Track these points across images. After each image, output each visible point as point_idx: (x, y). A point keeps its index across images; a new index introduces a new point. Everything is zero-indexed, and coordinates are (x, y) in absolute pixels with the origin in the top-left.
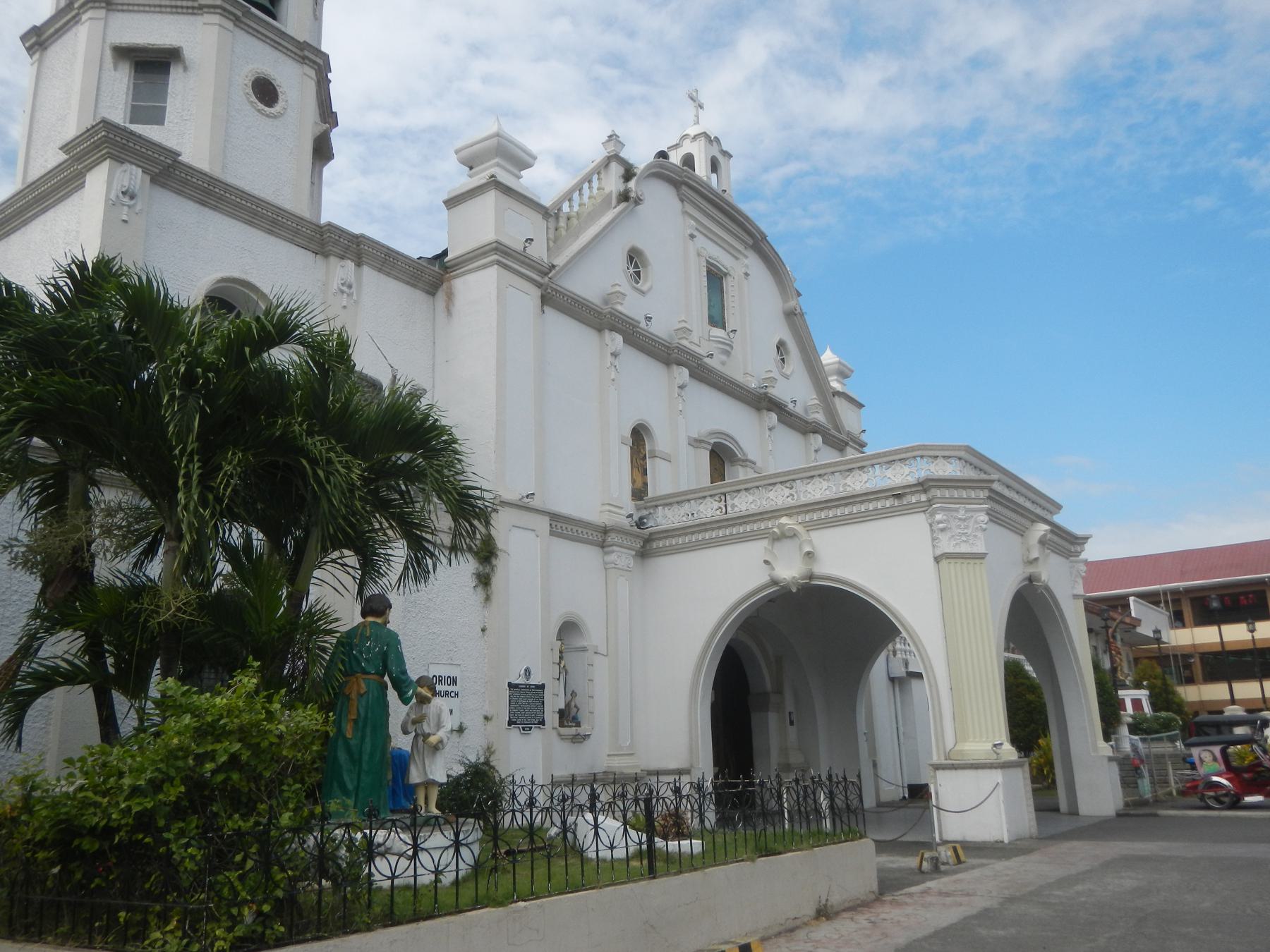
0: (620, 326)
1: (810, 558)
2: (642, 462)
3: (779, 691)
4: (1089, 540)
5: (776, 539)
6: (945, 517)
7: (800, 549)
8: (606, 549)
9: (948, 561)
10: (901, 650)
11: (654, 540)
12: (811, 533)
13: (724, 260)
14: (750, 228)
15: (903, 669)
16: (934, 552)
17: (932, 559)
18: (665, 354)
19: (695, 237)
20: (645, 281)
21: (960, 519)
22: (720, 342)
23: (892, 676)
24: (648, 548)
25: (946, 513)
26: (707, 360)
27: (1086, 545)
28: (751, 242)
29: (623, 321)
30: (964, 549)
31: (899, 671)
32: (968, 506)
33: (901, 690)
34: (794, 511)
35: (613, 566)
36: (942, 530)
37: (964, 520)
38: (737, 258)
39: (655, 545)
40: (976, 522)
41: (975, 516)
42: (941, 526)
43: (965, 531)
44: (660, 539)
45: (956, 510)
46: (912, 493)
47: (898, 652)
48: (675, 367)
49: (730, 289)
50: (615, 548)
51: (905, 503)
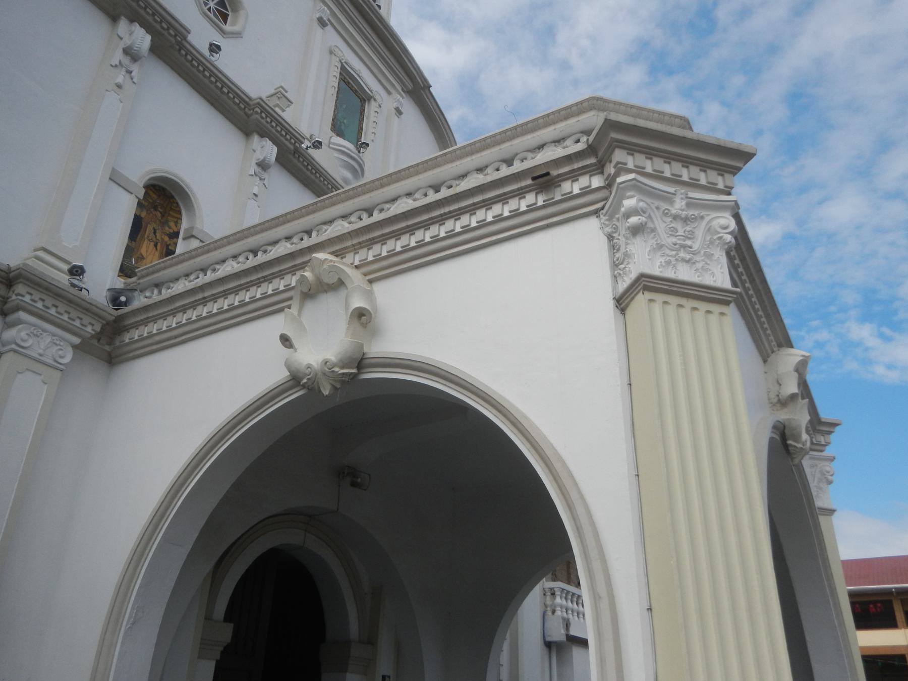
0: (150, 19)
1: (364, 325)
2: (166, 239)
3: (371, 641)
4: (837, 429)
5: (310, 294)
6: (641, 204)
7: (347, 308)
8: (11, 318)
9: (648, 295)
10: (561, 607)
11: (127, 329)
12: (378, 288)
13: (368, 80)
14: (409, 64)
15: (563, 631)
16: (614, 288)
17: (611, 304)
18: (242, 113)
19: (327, 25)
20: (234, 23)
21: (675, 217)
22: (343, 153)
23: (548, 639)
24: (117, 343)
25: (649, 200)
26: (314, 153)
27: (833, 437)
28: (410, 86)
29: (163, 19)
30: (684, 274)
31: (557, 634)
32: (692, 194)
33: (560, 661)
34: (349, 243)
35: (14, 346)
36: (636, 231)
37: (686, 220)
38: (389, 93)
39: (127, 338)
40: (709, 230)
41: (707, 219)
42: (634, 220)
43: (689, 243)
44: (136, 326)
45: (668, 198)
46: (573, 176)
47: (558, 609)
48: (256, 138)
49: (373, 114)
50: (22, 315)
51: (558, 197)
